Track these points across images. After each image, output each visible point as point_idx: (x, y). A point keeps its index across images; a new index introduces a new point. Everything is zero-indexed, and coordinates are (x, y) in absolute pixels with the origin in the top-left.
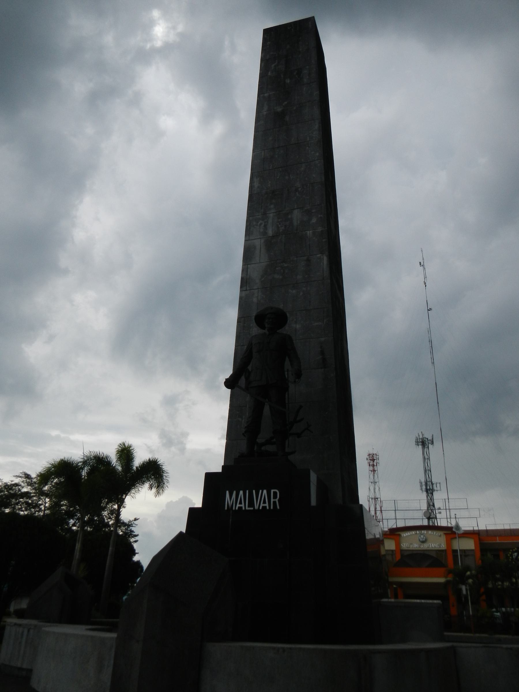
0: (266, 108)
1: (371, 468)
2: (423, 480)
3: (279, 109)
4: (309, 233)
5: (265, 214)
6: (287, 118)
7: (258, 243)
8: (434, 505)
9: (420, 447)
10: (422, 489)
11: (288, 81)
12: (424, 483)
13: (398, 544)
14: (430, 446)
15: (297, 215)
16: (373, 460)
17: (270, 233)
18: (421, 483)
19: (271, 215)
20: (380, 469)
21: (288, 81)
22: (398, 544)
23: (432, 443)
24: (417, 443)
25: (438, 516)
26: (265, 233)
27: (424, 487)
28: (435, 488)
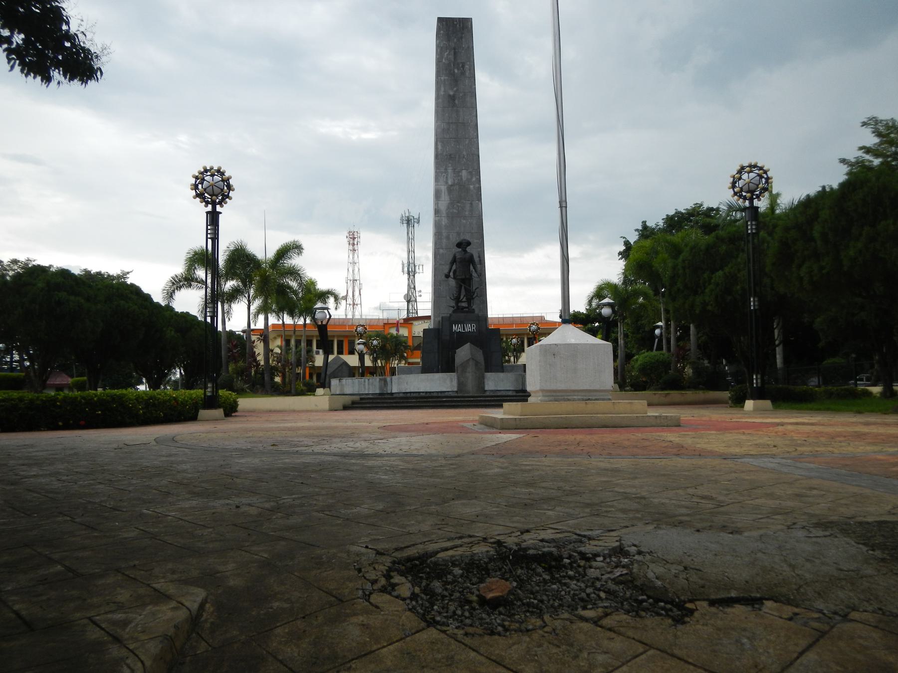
0: (442, 89)
1: (351, 247)
2: (406, 262)
3: (451, 93)
4: (472, 187)
5: (446, 169)
6: (456, 102)
7: (443, 188)
8: (414, 288)
9: (405, 225)
10: (403, 271)
11: (456, 71)
12: (406, 265)
13: (410, 332)
14: (416, 225)
15: (464, 173)
16: (354, 239)
17: (450, 183)
18: (403, 265)
19: (450, 170)
20: (360, 248)
21: (456, 71)
22: (410, 332)
23: (418, 222)
24: (402, 220)
25: (418, 299)
26: (447, 183)
27: (406, 269)
28: (417, 270)
